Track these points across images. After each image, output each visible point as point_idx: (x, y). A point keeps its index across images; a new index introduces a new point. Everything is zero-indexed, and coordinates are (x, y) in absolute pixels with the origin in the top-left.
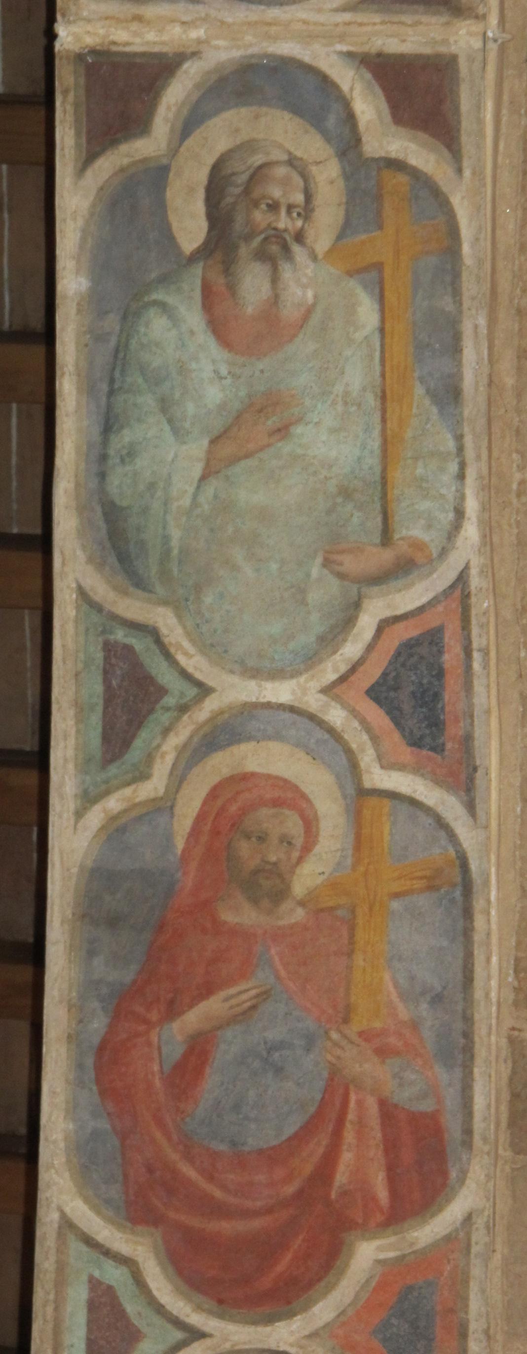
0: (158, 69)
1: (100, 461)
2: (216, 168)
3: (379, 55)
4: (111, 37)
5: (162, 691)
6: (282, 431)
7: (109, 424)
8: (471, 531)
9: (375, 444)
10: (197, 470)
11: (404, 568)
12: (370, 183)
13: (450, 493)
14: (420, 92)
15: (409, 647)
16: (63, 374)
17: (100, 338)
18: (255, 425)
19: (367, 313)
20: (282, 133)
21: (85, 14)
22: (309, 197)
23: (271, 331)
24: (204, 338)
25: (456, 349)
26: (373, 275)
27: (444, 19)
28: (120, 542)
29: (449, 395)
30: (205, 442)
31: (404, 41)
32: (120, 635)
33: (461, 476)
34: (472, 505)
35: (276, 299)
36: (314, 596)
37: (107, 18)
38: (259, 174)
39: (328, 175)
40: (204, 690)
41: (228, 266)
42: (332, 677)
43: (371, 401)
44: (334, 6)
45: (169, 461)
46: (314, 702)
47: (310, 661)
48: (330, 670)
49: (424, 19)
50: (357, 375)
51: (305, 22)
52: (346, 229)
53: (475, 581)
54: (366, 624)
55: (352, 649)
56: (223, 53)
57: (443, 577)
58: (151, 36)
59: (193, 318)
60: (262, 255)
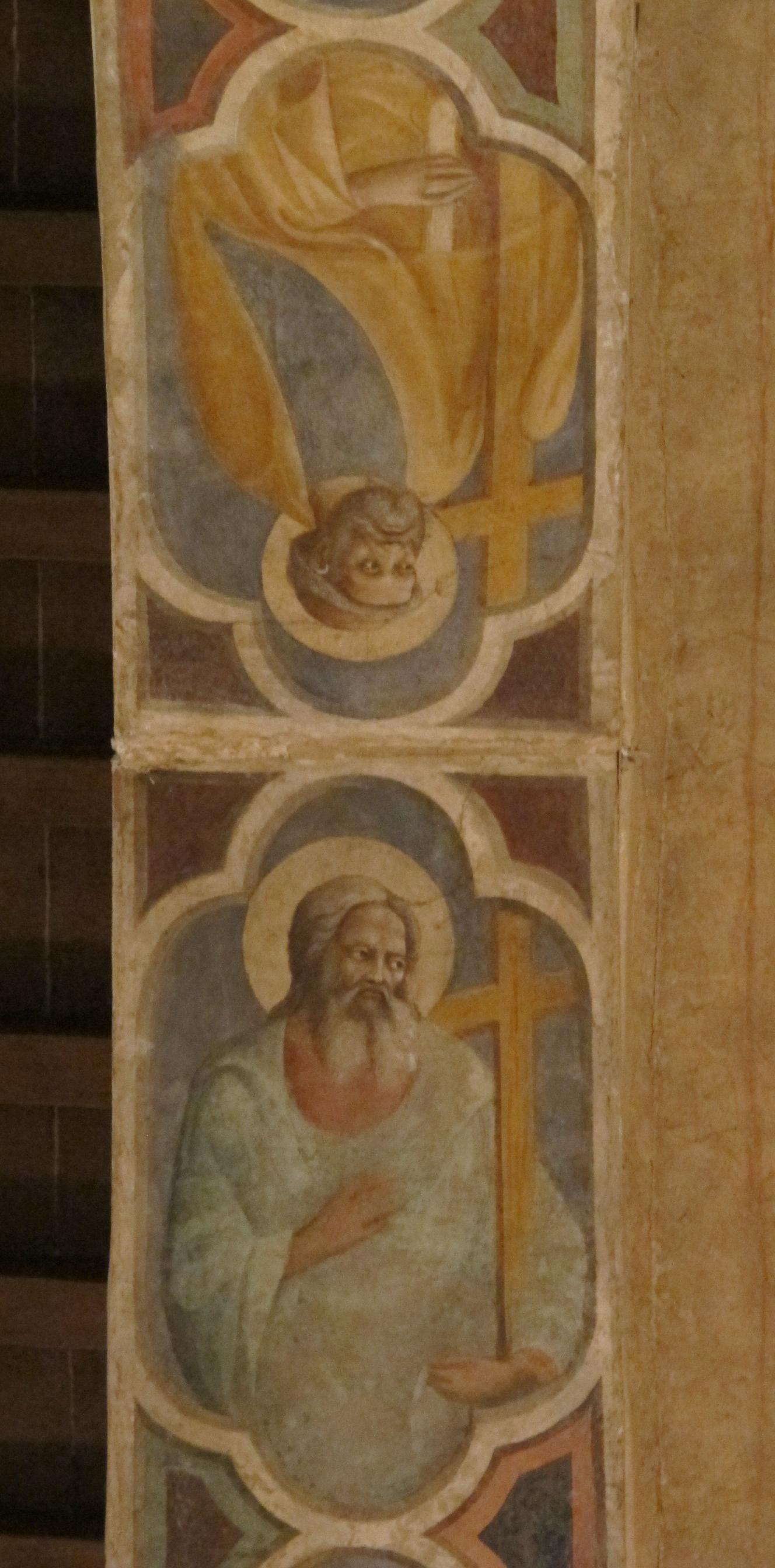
0: (233, 792)
1: (164, 1256)
2: (301, 911)
3: (495, 777)
4: (178, 755)
5: (238, 1535)
6: (380, 1222)
7: (174, 1211)
8: (603, 1342)
9: (490, 1238)
10: (278, 1269)
11: (524, 1387)
12: (480, 922)
13: (576, 1293)
14: (542, 820)
15: (529, 1482)
16: (120, 1153)
17: (162, 1109)
18: (347, 1215)
19: (480, 1082)
20: (379, 868)
21: (147, 727)
22: (411, 943)
23: (364, 1103)
24: (285, 1109)
25: (586, 1125)
26: (487, 1039)
27: (569, 736)
28: (189, 1356)
29: (577, 1180)
30: (288, 1234)
31: (522, 761)
32: (187, 1466)
33: (591, 1276)
34: (603, 1311)
35: (372, 1064)
36: (416, 1420)
37: (172, 733)
38: (351, 917)
39: (434, 919)
40: (287, 1532)
41: (316, 1026)
42: (437, 1516)
43: (485, 1187)
44: (442, 720)
45: (246, 1258)
46: (416, 1547)
47: (411, 1496)
48: (435, 1512)
49: (547, 735)
50: (467, 1157)
51: (406, 738)
52: (455, 982)
53: (609, 1403)
54: (479, 1453)
55: (462, 1484)
56: (307, 775)
57: (570, 1397)
58: (225, 753)
59: (274, 1086)
60: (356, 1012)
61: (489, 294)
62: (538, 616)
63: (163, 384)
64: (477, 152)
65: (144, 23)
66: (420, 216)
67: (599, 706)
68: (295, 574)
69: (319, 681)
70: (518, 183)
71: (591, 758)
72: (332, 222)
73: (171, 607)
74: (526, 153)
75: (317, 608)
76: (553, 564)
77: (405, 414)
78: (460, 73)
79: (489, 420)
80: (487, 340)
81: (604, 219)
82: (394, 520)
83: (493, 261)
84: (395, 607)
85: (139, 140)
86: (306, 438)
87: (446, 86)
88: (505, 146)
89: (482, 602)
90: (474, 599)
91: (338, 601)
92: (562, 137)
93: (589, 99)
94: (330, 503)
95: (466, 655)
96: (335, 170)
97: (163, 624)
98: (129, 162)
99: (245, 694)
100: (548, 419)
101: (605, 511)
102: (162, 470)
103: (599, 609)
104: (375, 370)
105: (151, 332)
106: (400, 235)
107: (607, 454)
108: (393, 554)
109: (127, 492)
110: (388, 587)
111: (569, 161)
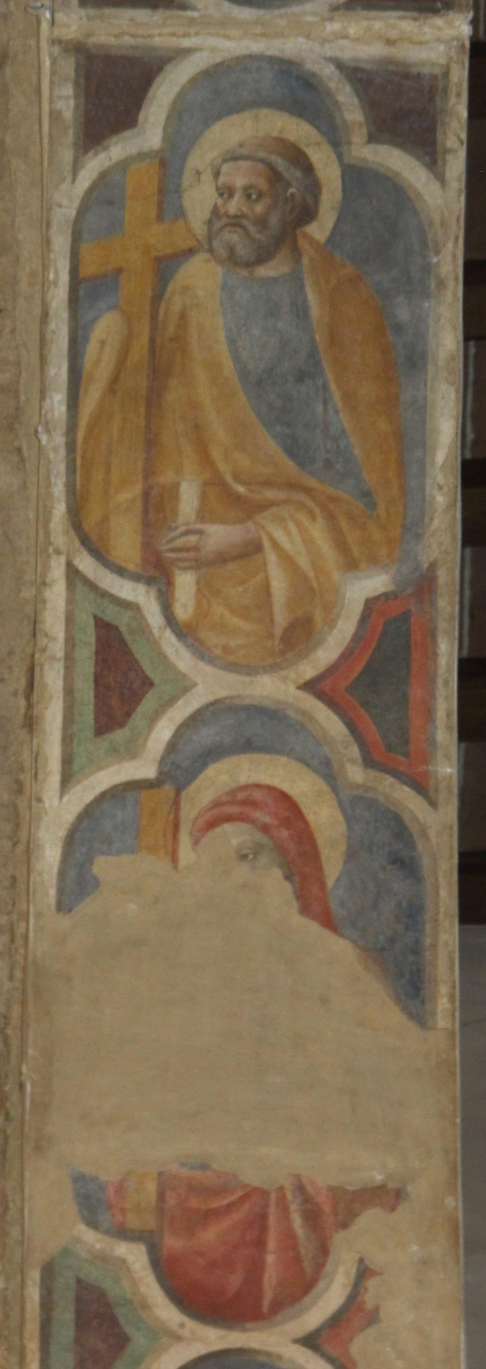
4: (417, 24)
21: (442, 48)
27: (92, 40)
31: (132, 20)
37: (421, 43)
44: (198, 55)
49: (112, 41)
51: (227, 37)
58: (378, 25)
61: (152, 443)
62: (118, 150)
63: (416, 360)
64: (157, 572)
65: (416, 692)
66: (204, 514)
67: (68, 66)
68: (314, 188)
69: (297, 89)
70: (126, 543)
71: (74, 23)
72: (274, 510)
73: (418, 158)
74: (120, 571)
75: (298, 158)
76: (104, 195)
77: (222, 335)
78: (170, 644)
79: (154, 329)
80: (153, 401)
81: (60, 510)
82: (233, 237)
83: (149, 472)
84: (234, 158)
85: (424, 585)
86: (301, 311)
87: (184, 632)
88: (136, 578)
89: (163, 163)
90: (168, 164)
91: (280, 163)
92: (92, 586)
93: (70, 619)
94: (284, 254)
95: (178, 113)
96: (271, 557)
97: (425, 144)
98: (433, 566)
99: (357, 75)
100: (106, 327)
101: (61, 243)
102: (418, 284)
103: (67, 155)
104: (244, 374)
105: (422, 409)
106: (223, 500)
107: (59, 297)
108: (234, 206)
109: (450, 261)
110: (239, 176)
111: (86, 564)
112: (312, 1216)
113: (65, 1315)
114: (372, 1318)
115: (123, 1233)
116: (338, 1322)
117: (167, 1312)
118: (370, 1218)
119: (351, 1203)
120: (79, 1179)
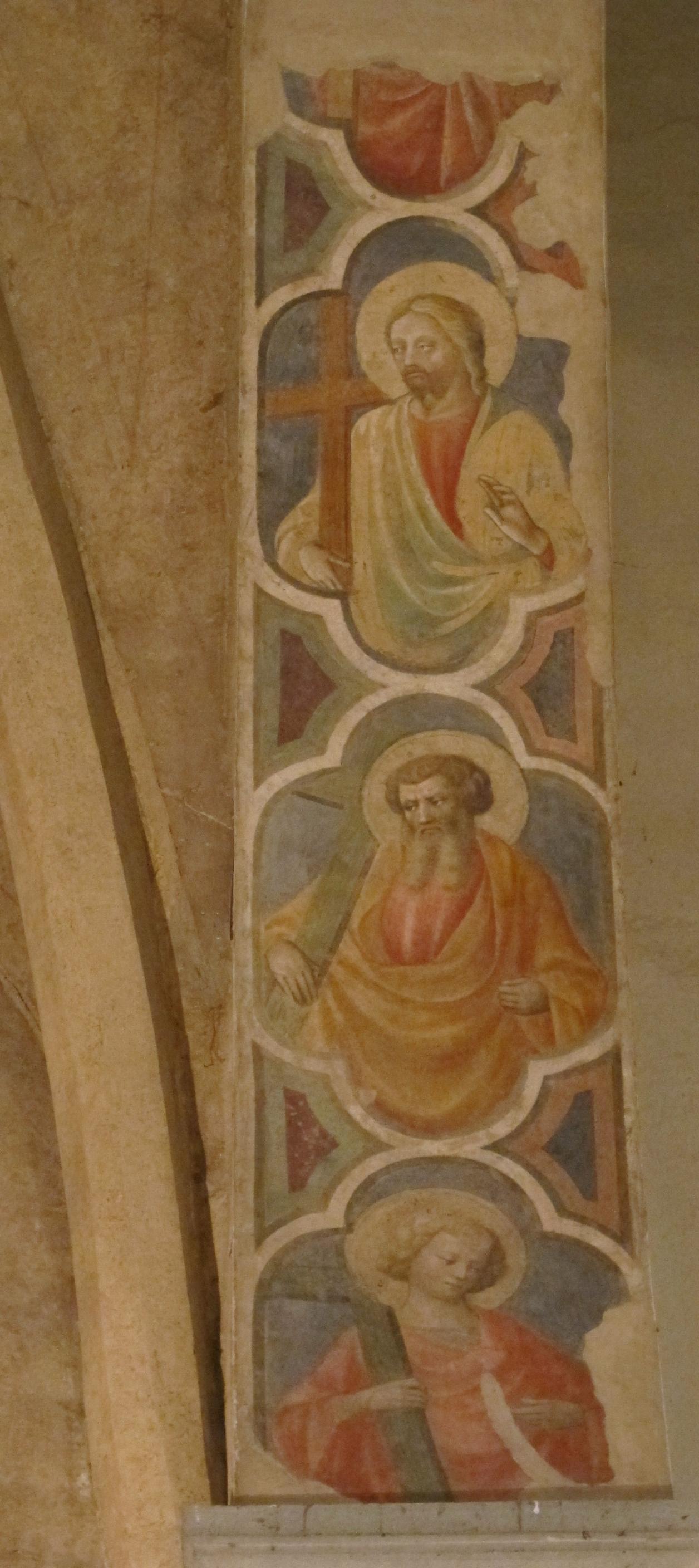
112: (481, 107)
113: (277, 187)
114: (531, 192)
115: (324, 121)
116: (501, 193)
117: (362, 187)
118: (529, 110)
119: (513, 97)
120: (288, 76)
